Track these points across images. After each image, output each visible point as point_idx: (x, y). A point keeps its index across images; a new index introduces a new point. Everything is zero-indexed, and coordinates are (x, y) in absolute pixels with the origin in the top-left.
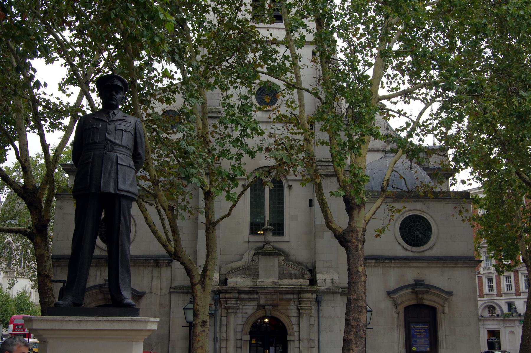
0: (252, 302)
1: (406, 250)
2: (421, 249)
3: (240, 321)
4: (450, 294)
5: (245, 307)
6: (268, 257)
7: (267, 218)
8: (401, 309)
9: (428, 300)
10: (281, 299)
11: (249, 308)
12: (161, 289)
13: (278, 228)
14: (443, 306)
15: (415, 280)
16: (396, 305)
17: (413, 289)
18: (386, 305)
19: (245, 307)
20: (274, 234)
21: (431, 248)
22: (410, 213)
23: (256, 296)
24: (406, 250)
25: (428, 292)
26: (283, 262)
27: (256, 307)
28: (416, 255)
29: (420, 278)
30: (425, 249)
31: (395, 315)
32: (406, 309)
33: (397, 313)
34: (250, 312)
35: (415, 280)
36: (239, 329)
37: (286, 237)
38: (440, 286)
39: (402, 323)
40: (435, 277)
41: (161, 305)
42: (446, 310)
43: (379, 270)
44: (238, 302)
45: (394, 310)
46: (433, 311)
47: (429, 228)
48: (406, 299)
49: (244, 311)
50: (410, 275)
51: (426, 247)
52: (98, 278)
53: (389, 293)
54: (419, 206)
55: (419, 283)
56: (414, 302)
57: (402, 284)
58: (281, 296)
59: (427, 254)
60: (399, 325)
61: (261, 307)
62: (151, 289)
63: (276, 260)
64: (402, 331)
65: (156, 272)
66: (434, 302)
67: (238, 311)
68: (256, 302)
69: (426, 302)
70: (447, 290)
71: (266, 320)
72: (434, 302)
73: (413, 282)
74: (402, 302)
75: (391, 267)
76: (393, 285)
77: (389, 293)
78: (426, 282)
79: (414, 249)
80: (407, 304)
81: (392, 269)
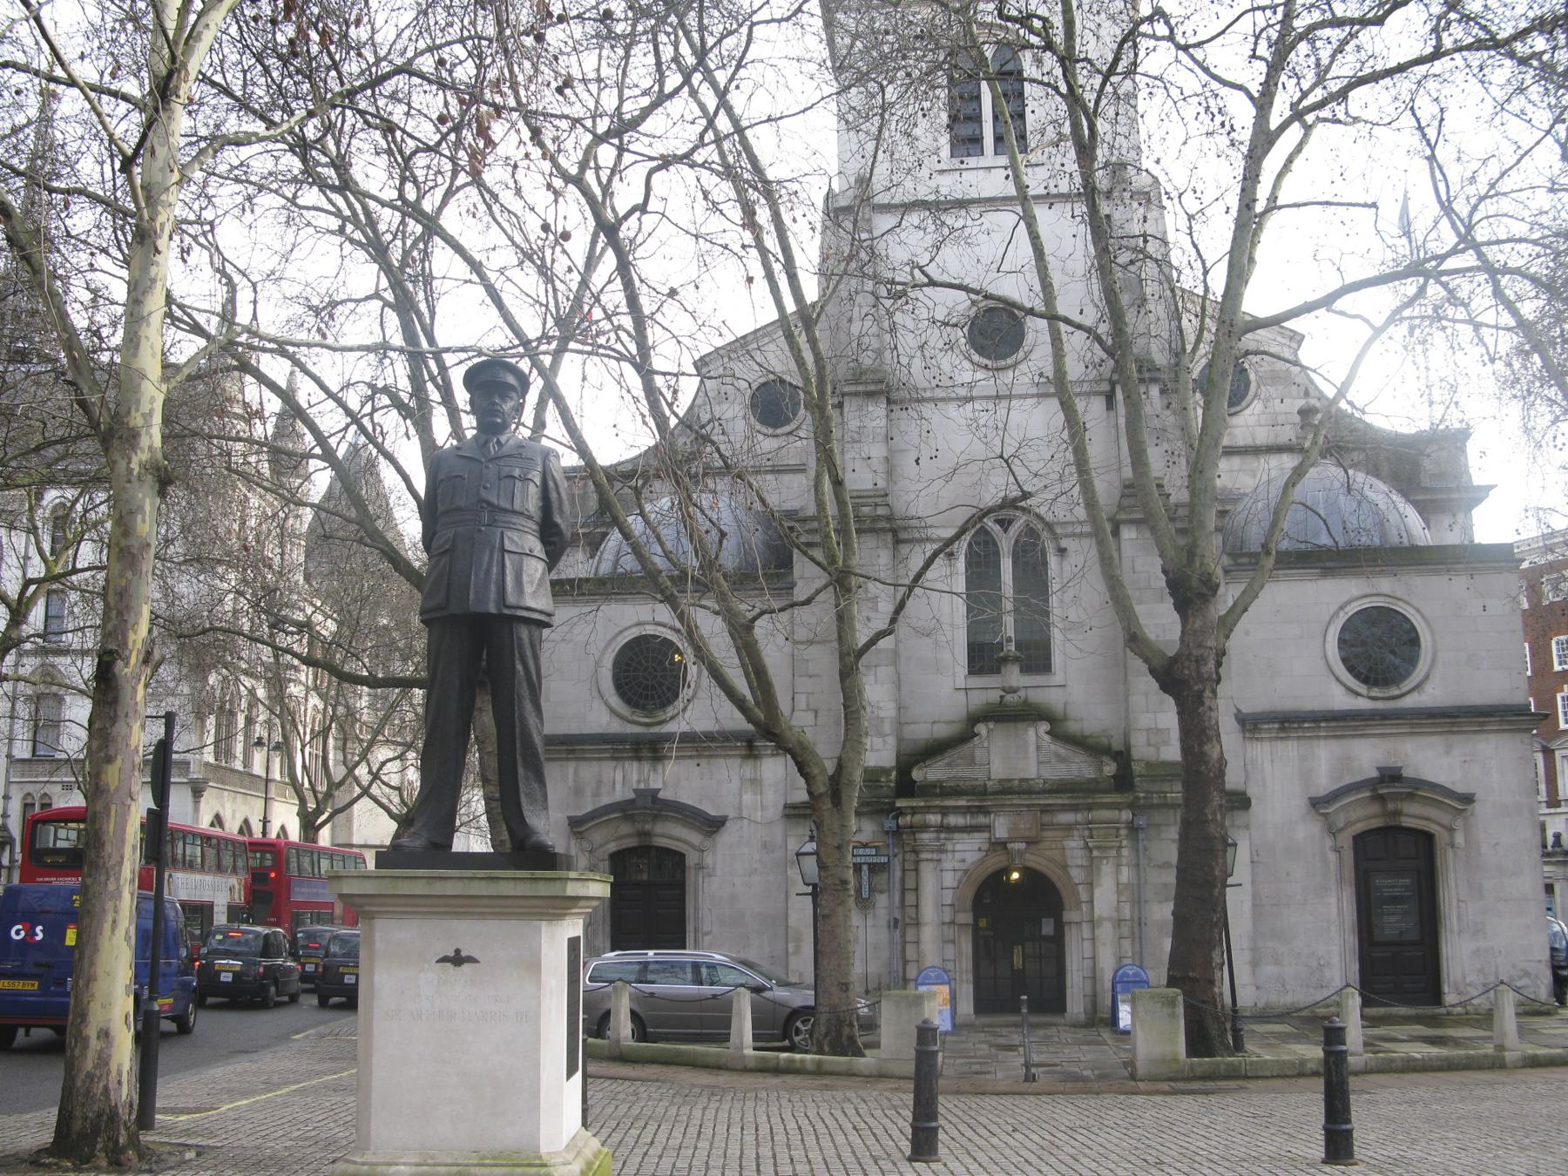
0: (976, 835)
1: (1358, 694)
2: (1395, 692)
3: (949, 879)
4: (1468, 799)
5: (958, 847)
6: (1012, 725)
7: (1011, 633)
8: (1346, 840)
9: (1414, 815)
10: (1044, 826)
11: (967, 851)
12: (763, 809)
13: (1036, 658)
14: (1451, 830)
15: (1379, 769)
16: (1333, 832)
17: (1374, 790)
18: (1308, 831)
19: (958, 847)
20: (1027, 669)
21: (1418, 687)
22: (1366, 604)
23: (982, 820)
24: (1358, 694)
25: (1411, 797)
26: (1047, 738)
27: (985, 846)
28: (1380, 705)
29: (1392, 762)
30: (1404, 689)
31: (1332, 857)
32: (1360, 840)
33: (1337, 850)
34: (972, 857)
35: (1379, 769)
36: (948, 897)
37: (1058, 677)
38: (1442, 779)
39: (1349, 873)
40: (1430, 759)
41: (765, 846)
42: (1459, 839)
43: (1289, 750)
44: (943, 835)
45: (1329, 842)
46: (1426, 840)
47: (1415, 641)
48: (1361, 816)
49: (958, 856)
50: (1368, 755)
51: (1407, 685)
52: (618, 786)
53: (1317, 803)
54: (1385, 584)
56: (1376, 823)
57: (1348, 780)
58: (1047, 818)
59: (1410, 702)
60: (1341, 881)
61: (999, 845)
62: (740, 809)
63: (1031, 732)
64: (1349, 894)
65: (748, 769)
66: (1428, 819)
67: (944, 856)
68: (986, 835)
71: (1015, 876)
72: (1428, 819)
73: (1374, 774)
74: (1349, 824)
75: (1318, 737)
76: (1324, 783)
77: (1316, 803)
78: (1408, 773)
79: (1375, 692)
80: (1360, 827)
81: (1322, 742)
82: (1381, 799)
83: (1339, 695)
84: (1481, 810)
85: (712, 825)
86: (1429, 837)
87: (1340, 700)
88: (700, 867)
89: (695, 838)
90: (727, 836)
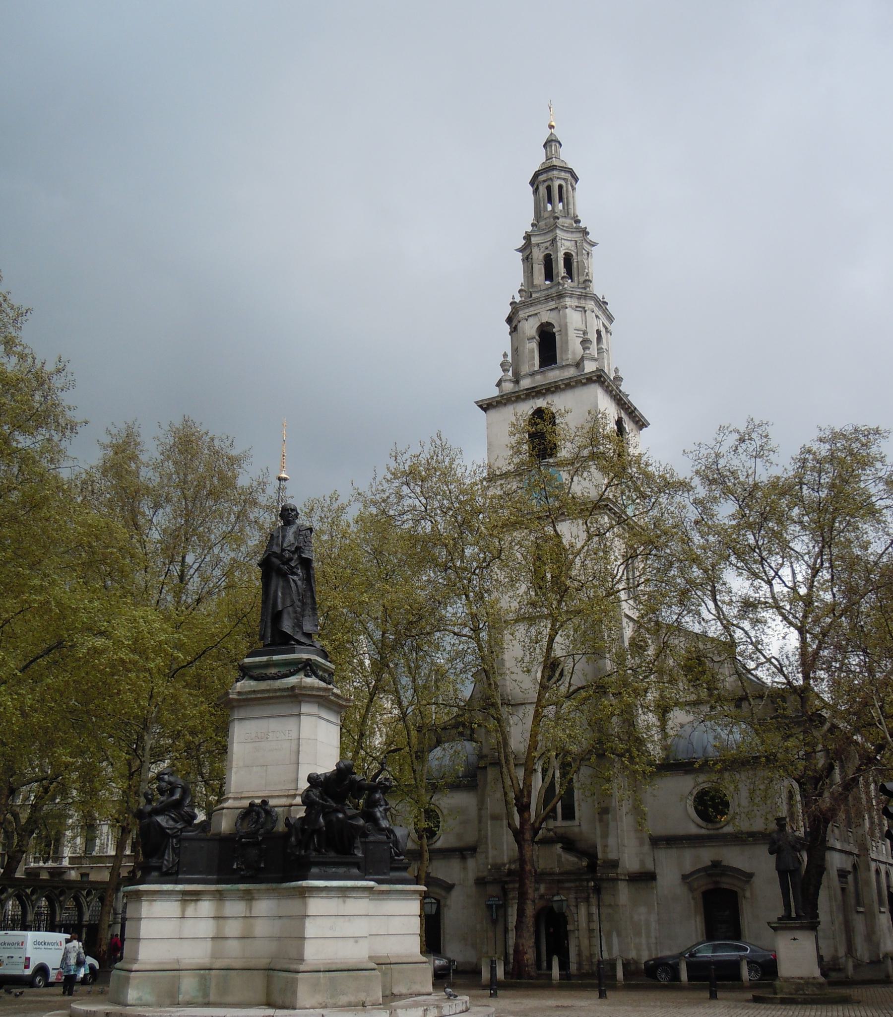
4: (750, 876)
9: (726, 883)
14: (744, 890)
16: (691, 890)
28: (712, 832)
31: (692, 902)
33: (694, 899)
40: (735, 858)
42: (748, 894)
43: (674, 852)
53: (684, 877)
55: (716, 864)
56: (711, 887)
57: (699, 866)
69: (725, 886)
70: (748, 870)
73: (710, 863)
76: (688, 868)
77: (684, 877)
78: (724, 863)
79: (710, 826)
80: (704, 888)
82: (709, 875)
83: (692, 826)
84: (757, 881)
85: (449, 888)
86: (735, 893)
87: (693, 830)
88: (445, 906)
89: (443, 893)
90: (455, 893)
